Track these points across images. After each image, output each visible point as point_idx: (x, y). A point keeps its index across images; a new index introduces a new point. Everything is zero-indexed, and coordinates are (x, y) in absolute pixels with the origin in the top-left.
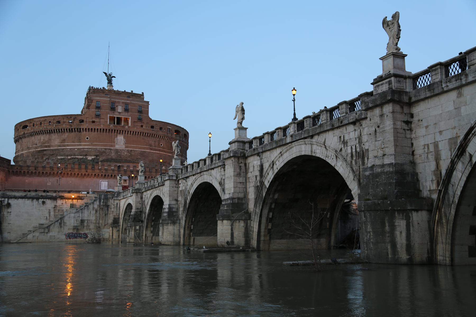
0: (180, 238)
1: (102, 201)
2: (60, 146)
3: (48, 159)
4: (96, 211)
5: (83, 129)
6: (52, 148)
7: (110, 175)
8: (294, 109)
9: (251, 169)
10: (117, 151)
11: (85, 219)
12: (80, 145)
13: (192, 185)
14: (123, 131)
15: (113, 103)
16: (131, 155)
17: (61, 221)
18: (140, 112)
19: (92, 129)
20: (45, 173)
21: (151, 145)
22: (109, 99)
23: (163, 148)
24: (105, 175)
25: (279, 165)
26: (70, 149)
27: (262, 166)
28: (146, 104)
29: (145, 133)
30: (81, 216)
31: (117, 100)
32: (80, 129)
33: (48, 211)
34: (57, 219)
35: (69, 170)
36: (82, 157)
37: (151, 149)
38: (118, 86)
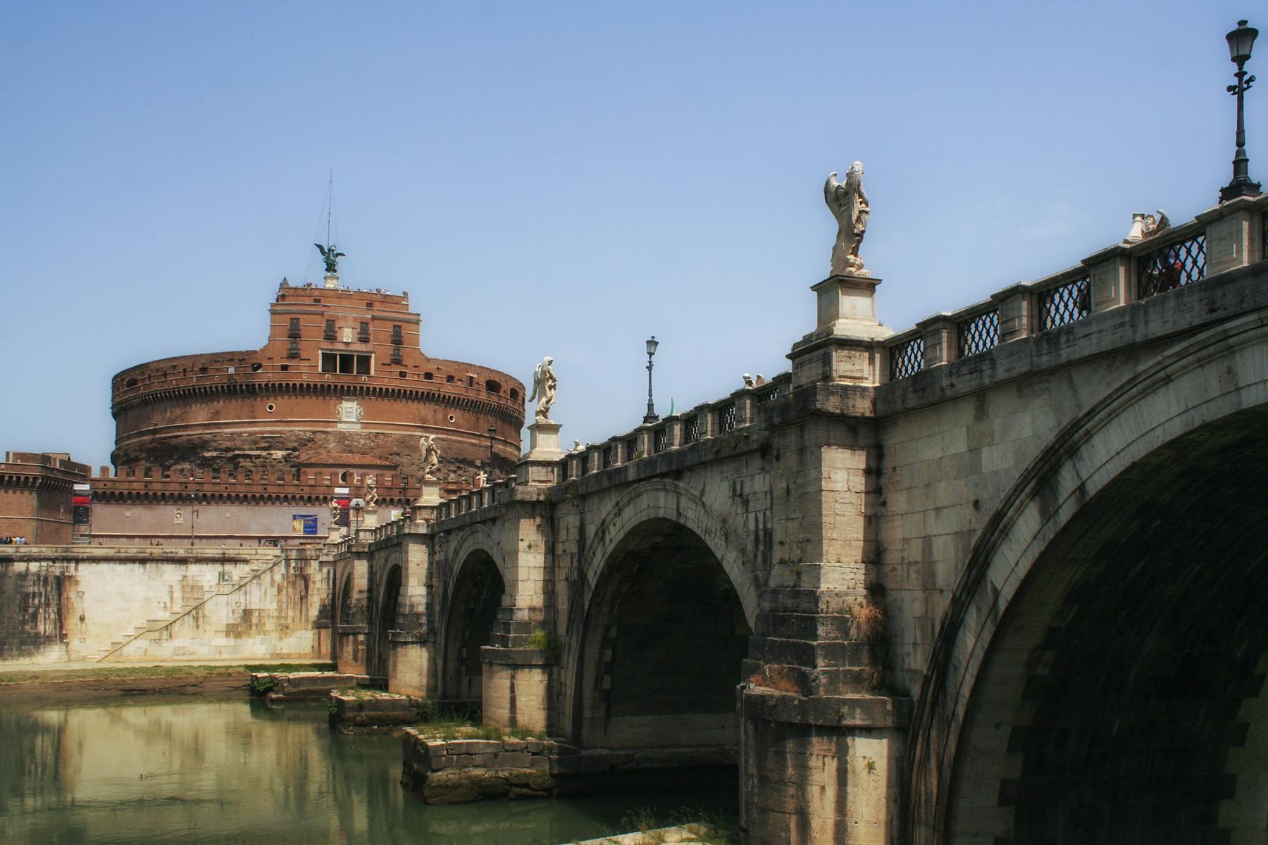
0: (436, 678)
1: (293, 564)
4: (280, 591)
7: (321, 497)
8: (650, 390)
9: (563, 535)
10: (342, 437)
11: (253, 607)
13: (457, 552)
16: (379, 446)
17: (196, 612)
25: (616, 534)
27: (582, 530)
30: (243, 600)
33: (167, 589)
34: (189, 609)
35: (223, 487)
36: (258, 452)
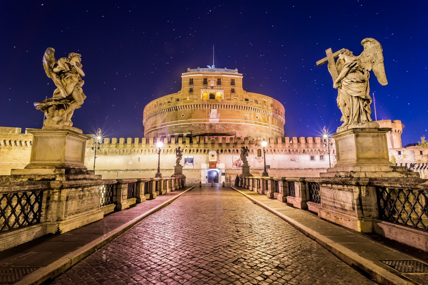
2: (162, 126)
6: (157, 128)
7: (195, 150)
10: (211, 126)
12: (177, 123)
14: (216, 105)
20: (125, 150)
22: (202, 75)
32: (176, 107)
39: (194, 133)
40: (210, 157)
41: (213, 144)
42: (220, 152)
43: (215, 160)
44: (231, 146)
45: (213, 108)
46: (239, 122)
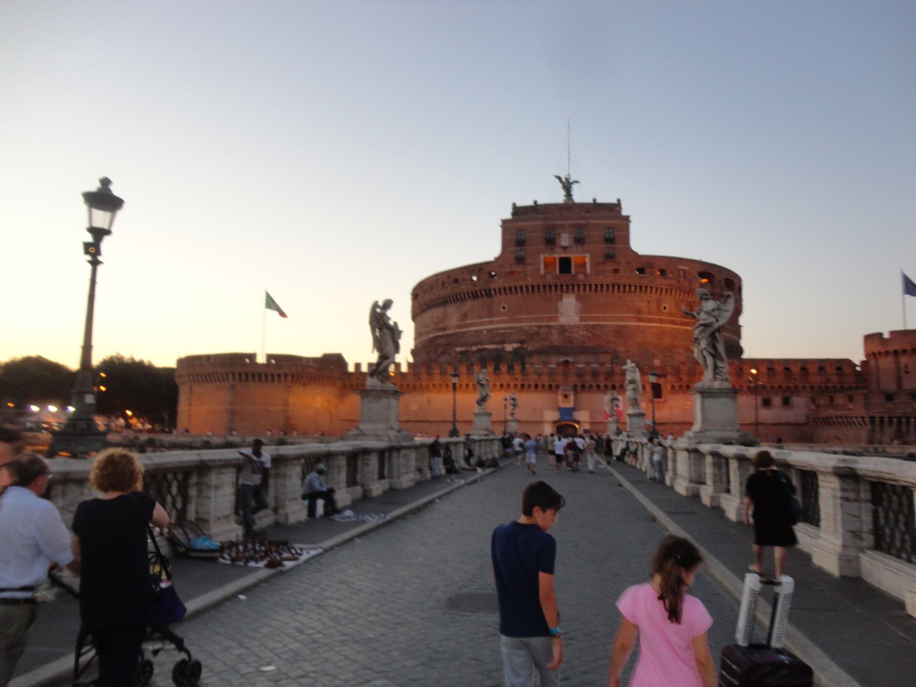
2: (459, 327)
3: (443, 353)
5: (495, 290)
6: (448, 332)
7: (533, 384)
10: (563, 329)
12: (491, 323)
14: (573, 286)
15: (551, 228)
18: (610, 240)
19: (510, 288)
21: (639, 311)
22: (540, 223)
23: (671, 314)
24: (523, 386)
26: (475, 332)
28: (624, 222)
29: (624, 286)
31: (558, 222)
32: (490, 290)
37: (640, 320)
38: (581, 196)
39: (530, 348)
40: (560, 398)
41: (566, 375)
42: (579, 388)
43: (570, 404)
44: (602, 378)
45: (567, 291)
46: (623, 320)
